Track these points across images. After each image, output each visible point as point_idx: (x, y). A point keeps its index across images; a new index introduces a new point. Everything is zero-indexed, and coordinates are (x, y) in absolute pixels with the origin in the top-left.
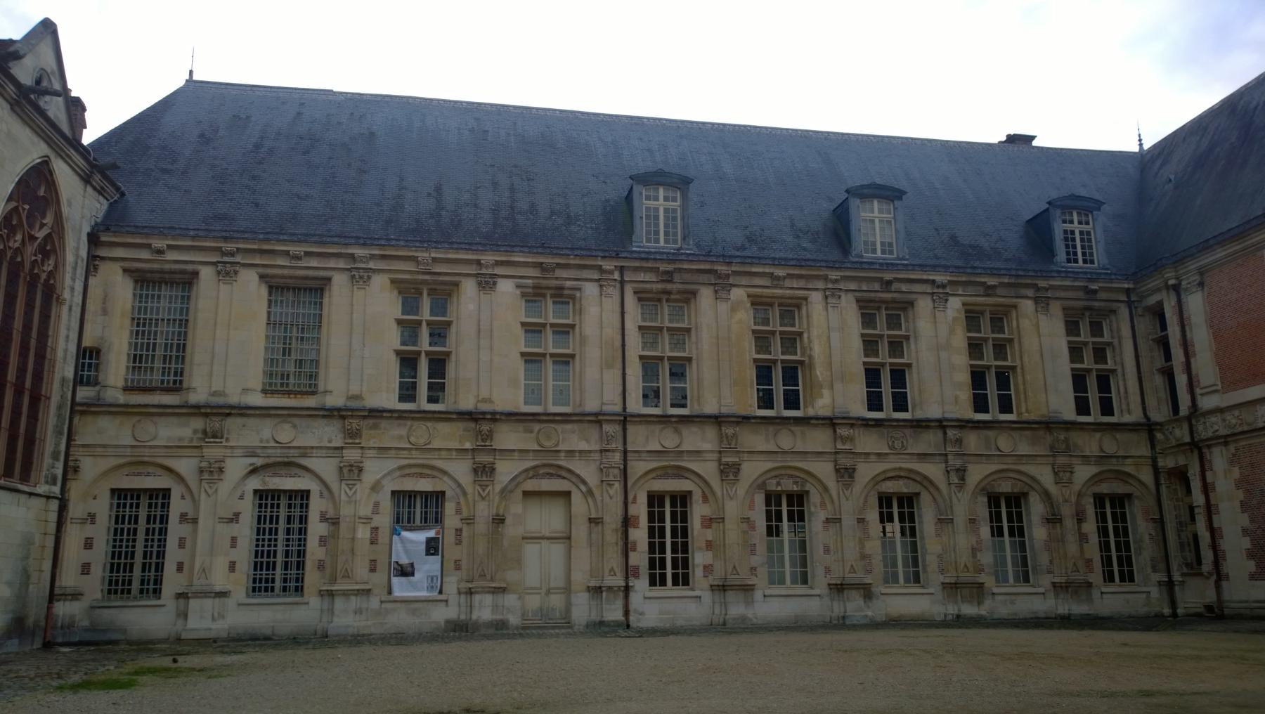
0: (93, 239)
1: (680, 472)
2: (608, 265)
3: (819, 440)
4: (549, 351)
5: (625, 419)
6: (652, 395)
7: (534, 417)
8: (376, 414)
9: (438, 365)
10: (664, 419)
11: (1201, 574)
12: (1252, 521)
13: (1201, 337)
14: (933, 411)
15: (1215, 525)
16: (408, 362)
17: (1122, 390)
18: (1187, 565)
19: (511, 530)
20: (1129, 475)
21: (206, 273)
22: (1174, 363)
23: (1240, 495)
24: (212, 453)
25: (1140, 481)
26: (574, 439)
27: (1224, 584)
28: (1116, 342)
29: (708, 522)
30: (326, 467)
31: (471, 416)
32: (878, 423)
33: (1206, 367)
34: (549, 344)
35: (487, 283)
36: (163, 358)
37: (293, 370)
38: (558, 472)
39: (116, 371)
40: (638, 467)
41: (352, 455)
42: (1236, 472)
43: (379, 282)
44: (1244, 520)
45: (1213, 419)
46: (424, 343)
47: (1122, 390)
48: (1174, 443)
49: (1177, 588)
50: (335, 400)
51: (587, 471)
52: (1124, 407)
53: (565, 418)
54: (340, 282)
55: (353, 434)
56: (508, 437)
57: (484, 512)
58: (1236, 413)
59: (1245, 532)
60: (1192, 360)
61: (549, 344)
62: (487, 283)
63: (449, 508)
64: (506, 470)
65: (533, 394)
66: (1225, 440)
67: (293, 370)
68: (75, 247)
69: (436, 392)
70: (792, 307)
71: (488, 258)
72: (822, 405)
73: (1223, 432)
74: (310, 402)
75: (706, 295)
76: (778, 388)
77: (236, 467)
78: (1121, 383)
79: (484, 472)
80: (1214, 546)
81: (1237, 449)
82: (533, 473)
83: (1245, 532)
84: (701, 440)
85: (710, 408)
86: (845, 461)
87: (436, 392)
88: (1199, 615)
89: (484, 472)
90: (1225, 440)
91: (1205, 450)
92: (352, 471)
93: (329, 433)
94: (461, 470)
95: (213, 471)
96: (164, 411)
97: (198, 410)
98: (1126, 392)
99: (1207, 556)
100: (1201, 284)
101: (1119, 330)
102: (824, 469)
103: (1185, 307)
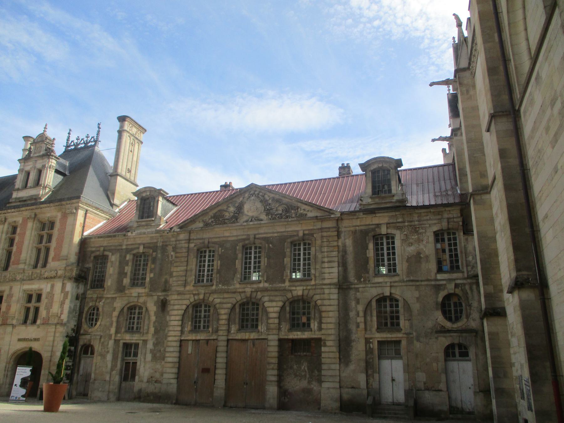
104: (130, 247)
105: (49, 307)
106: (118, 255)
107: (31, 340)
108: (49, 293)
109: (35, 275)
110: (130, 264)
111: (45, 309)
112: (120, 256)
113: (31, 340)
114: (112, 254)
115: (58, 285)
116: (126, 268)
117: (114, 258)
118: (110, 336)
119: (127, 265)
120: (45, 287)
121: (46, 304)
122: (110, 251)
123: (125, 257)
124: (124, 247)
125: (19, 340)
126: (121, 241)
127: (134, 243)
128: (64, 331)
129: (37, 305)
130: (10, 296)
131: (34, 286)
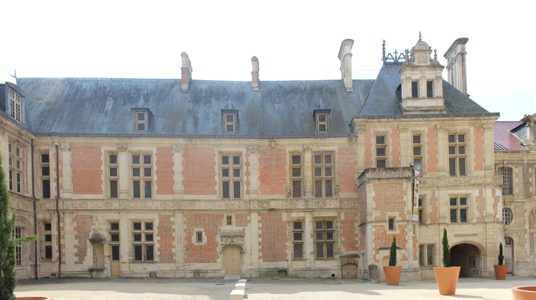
11: (52, 262)
12: (79, 242)
13: (67, 170)
15: (61, 243)
17: (25, 182)
18: (42, 258)
20: (26, 219)
22: (51, 177)
23: (76, 233)
25: (29, 222)
27: (62, 265)
28: (25, 160)
33: (67, 181)
42: (75, 224)
44: (76, 242)
45: (68, 203)
47: (25, 182)
48: (45, 209)
49: (38, 267)
52: (25, 190)
58: (79, 202)
59: (75, 246)
60: (60, 178)
66: (72, 212)
73: (71, 208)
78: (25, 179)
80: (60, 251)
81: (77, 216)
83: (75, 246)
88: (48, 278)
90: (72, 212)
91: (61, 214)
98: (27, 183)
99: (55, 254)
100: (70, 149)
101: (27, 155)
103: (60, 155)
104: (530, 162)
105: (481, 209)
106: (521, 168)
107: (468, 235)
108: (477, 197)
109: (459, 182)
110: (534, 176)
111: (477, 210)
112: (523, 169)
113: (468, 235)
114: (516, 167)
115: (488, 192)
116: (530, 179)
117: (516, 171)
118: (525, 231)
119: (531, 176)
120: (474, 193)
121: (478, 206)
122: (512, 164)
123: (528, 170)
124: (526, 162)
125: (456, 236)
126: (520, 157)
127: (533, 159)
128: (502, 227)
129: (463, 207)
130: (434, 199)
131: (460, 192)
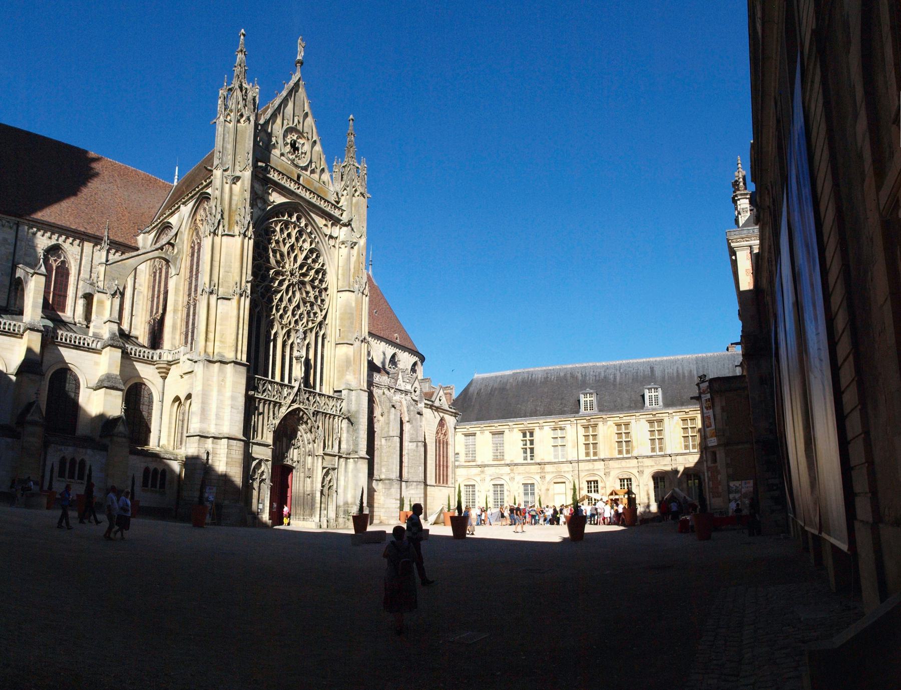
0: (455, 428)
1: (595, 475)
2: (572, 419)
3: (634, 462)
4: (559, 444)
5: (578, 461)
6: (587, 454)
7: (555, 463)
8: (516, 465)
9: (532, 450)
10: (589, 461)
14: (668, 452)
16: (525, 452)
19: (551, 492)
21: (478, 433)
24: (483, 476)
26: (567, 467)
29: (602, 488)
30: (507, 478)
31: (539, 464)
32: (589, 461)
34: (559, 442)
35: (541, 428)
36: (471, 454)
37: (499, 455)
38: (562, 477)
39: (462, 458)
40: (582, 474)
41: (512, 475)
43: (516, 430)
46: (528, 445)
50: (508, 462)
51: (569, 476)
53: (563, 463)
54: (507, 431)
55: (512, 470)
56: (548, 468)
57: (544, 488)
61: (559, 442)
62: (541, 428)
63: (536, 487)
64: (548, 477)
65: (556, 456)
67: (499, 455)
68: (451, 431)
69: (532, 457)
70: (627, 425)
71: (541, 421)
72: (635, 454)
74: (503, 462)
75: (600, 424)
76: (591, 451)
77: (488, 479)
79: (543, 478)
82: (556, 477)
84: (600, 465)
85: (602, 457)
86: (641, 469)
87: (532, 457)
89: (543, 478)
92: (512, 479)
93: (507, 469)
94: (537, 477)
95: (483, 480)
96: (472, 466)
97: (479, 466)
102: (635, 471)
